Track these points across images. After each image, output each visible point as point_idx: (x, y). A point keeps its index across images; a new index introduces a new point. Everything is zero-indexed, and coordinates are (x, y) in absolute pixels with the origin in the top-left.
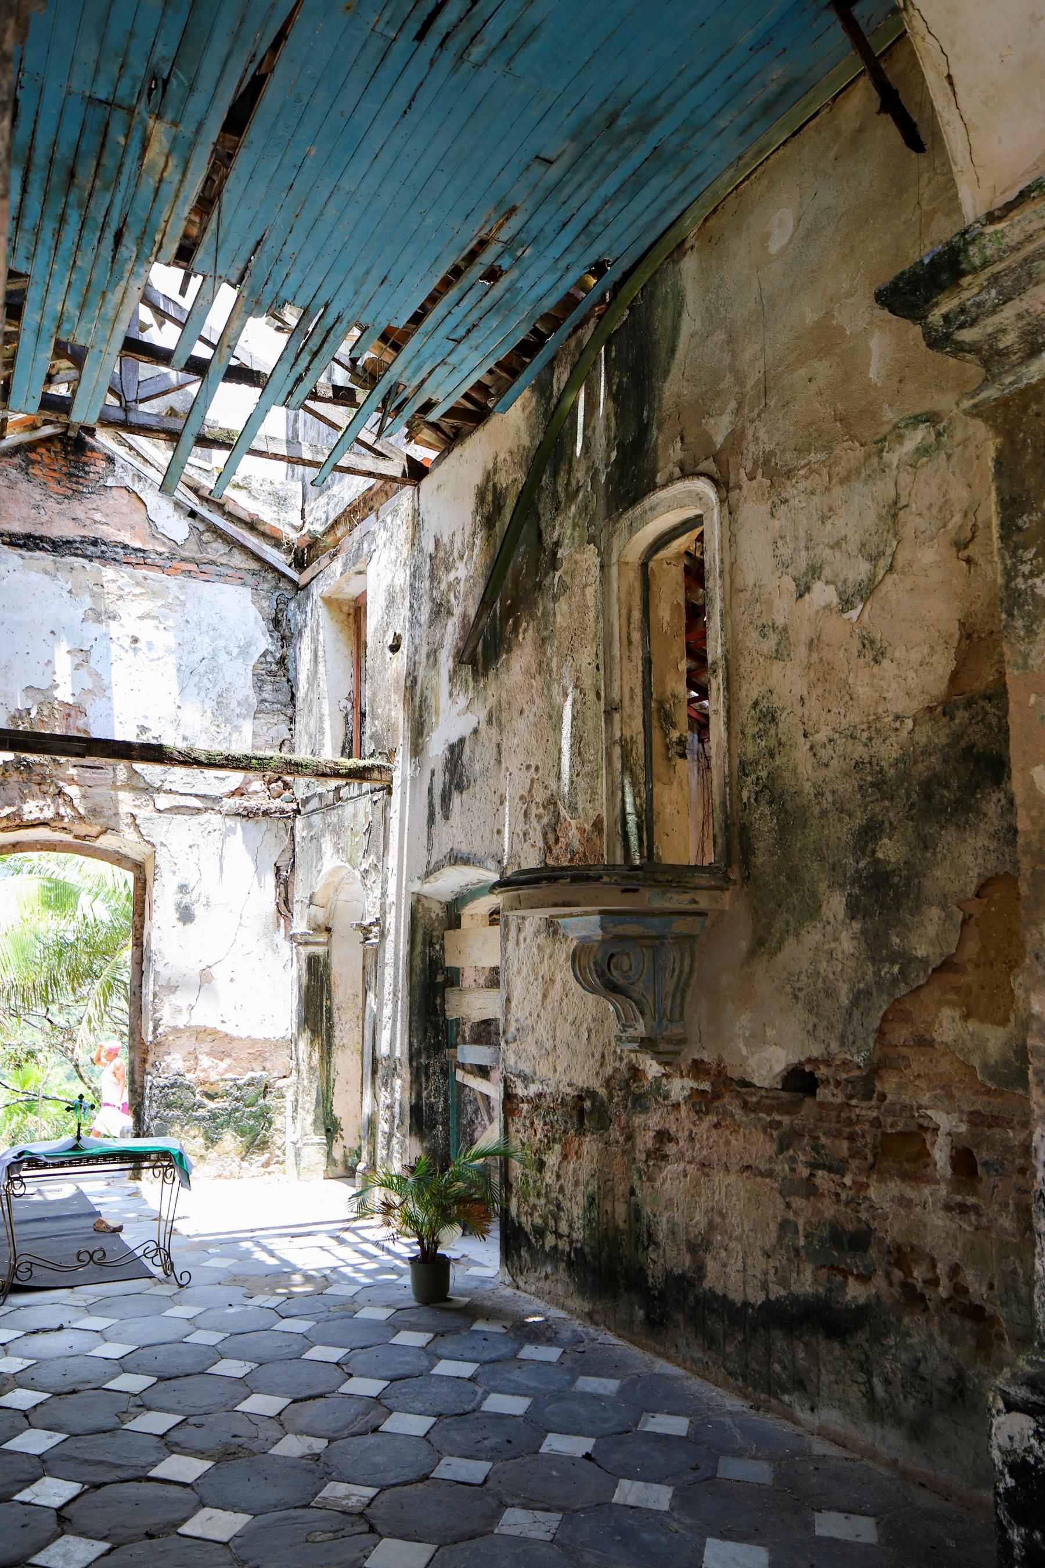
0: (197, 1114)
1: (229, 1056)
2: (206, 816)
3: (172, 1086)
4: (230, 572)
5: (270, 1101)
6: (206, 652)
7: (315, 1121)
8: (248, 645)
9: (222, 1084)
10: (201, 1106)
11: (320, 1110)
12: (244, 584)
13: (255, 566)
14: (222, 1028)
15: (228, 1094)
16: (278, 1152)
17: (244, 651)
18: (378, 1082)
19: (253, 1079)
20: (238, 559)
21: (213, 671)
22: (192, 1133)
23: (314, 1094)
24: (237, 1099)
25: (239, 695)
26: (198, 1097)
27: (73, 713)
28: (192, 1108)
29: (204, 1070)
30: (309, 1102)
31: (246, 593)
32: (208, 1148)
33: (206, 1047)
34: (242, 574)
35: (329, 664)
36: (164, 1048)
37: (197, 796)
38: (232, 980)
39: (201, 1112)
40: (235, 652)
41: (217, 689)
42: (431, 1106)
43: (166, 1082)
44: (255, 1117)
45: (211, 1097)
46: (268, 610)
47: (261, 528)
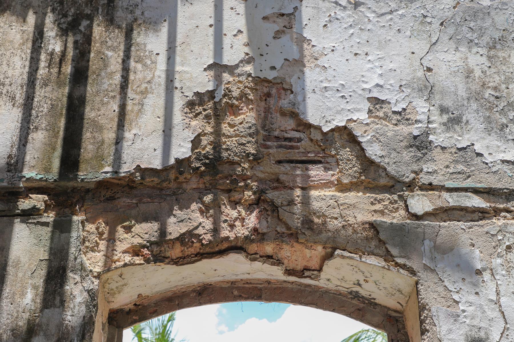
27: (274, 91)
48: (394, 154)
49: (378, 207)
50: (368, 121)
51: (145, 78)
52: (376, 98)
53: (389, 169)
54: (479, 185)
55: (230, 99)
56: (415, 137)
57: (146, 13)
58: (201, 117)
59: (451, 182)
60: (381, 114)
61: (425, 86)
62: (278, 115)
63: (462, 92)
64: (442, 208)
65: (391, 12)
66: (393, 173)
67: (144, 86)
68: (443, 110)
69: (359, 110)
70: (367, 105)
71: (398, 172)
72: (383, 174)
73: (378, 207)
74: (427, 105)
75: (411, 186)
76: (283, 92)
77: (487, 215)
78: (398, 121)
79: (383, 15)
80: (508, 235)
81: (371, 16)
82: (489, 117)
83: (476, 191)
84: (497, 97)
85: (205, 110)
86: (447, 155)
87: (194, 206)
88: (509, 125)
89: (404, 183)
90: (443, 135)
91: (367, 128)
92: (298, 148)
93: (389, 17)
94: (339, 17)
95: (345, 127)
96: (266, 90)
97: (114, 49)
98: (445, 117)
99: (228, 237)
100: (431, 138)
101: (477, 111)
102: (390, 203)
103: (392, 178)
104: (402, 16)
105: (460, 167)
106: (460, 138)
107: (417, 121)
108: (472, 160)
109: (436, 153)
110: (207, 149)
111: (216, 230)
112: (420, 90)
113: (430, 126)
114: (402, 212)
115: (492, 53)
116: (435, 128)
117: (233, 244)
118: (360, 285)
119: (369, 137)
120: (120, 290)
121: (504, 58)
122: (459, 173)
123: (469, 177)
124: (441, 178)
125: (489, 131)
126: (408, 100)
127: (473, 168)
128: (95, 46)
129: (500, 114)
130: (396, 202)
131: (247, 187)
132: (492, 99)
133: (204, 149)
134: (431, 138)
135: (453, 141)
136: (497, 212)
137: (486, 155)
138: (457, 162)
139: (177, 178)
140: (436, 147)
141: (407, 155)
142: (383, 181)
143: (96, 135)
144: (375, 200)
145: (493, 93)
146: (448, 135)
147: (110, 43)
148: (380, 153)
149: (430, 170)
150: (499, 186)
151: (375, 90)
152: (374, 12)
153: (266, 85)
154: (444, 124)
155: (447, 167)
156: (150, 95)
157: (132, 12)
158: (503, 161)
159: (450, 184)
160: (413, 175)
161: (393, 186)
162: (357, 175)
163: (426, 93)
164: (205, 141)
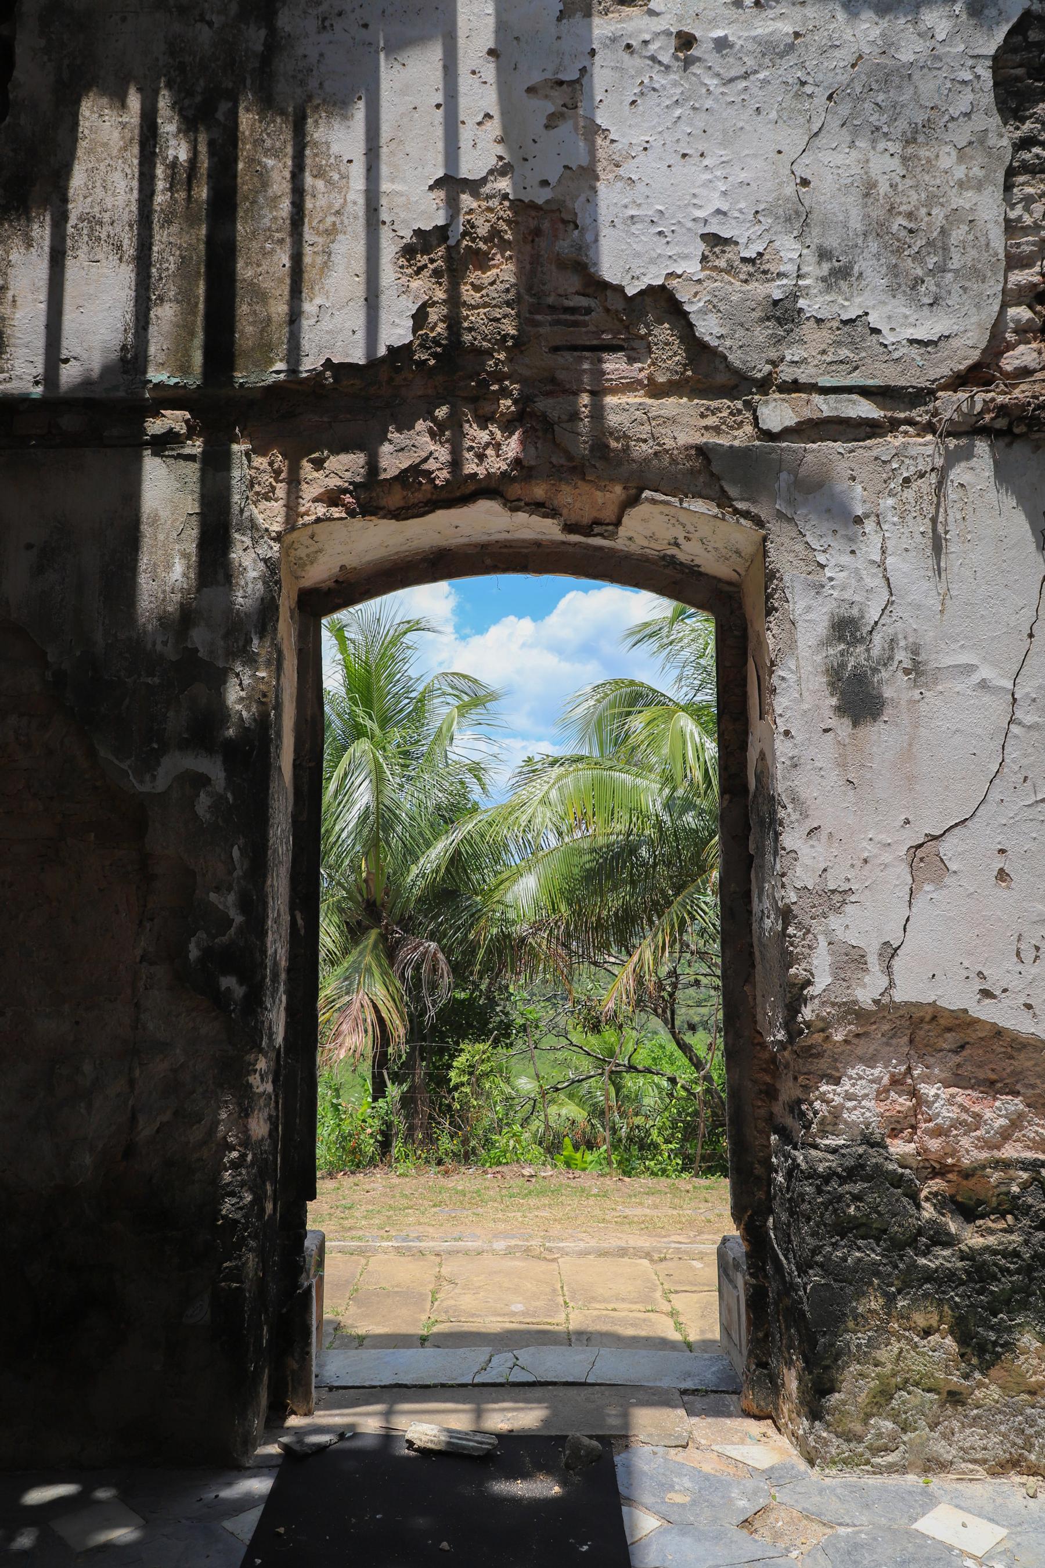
2: (895, 441)
3: (853, 1173)
9: (995, 1177)
14: (987, 1012)
22: (920, 1320)
26: (928, 1212)
27: (546, 225)
28: (912, 1242)
29: (938, 1132)
36: (823, 1064)
38: (1002, 875)
39: (941, 1258)
43: (831, 1162)
45: (969, 1212)
48: (740, 333)
49: (712, 421)
50: (701, 276)
51: (330, 206)
52: (715, 235)
53: (731, 357)
54: (870, 382)
55: (473, 240)
56: (776, 303)
57: (326, 84)
58: (426, 273)
59: (827, 377)
60: (722, 263)
61: (797, 212)
62: (553, 267)
63: (856, 224)
64: (810, 420)
65: (746, 76)
66: (737, 364)
67: (330, 219)
68: (824, 255)
69: (686, 257)
70: (701, 247)
71: (744, 363)
72: (722, 367)
73: (712, 421)
74: (798, 246)
75: (764, 385)
76: (561, 226)
77: (878, 430)
78: (750, 275)
79: (732, 80)
80: (907, 461)
81: (712, 82)
82: (896, 266)
83: (865, 392)
84: (911, 231)
85: (432, 261)
86: (825, 333)
87: (421, 425)
88: (926, 279)
89: (754, 380)
90: (820, 299)
91: (698, 287)
92: (585, 324)
93: (744, 84)
94: (657, 86)
95: (663, 287)
96: (532, 224)
97: (275, 153)
98: (826, 267)
99: (476, 474)
100: (802, 303)
101: (877, 256)
102: (731, 414)
103: (736, 372)
104: (765, 82)
105: (844, 353)
106: (846, 303)
107: (780, 275)
108: (863, 340)
109: (808, 329)
110: (438, 329)
111: (456, 463)
112: (788, 220)
113: (800, 283)
114: (749, 429)
115: (910, 150)
116: (807, 287)
117: (484, 484)
118: (677, 545)
119: (701, 304)
120: (312, 559)
121: (929, 161)
122: (841, 362)
123: (856, 368)
124: (812, 371)
125: (893, 290)
126: (767, 238)
127: (864, 354)
128: (246, 149)
129: (913, 261)
130: (739, 412)
131: (505, 393)
132: (903, 233)
133: (432, 329)
134: (802, 303)
135: (836, 309)
136: (894, 425)
137: (885, 331)
138: (838, 343)
139: (391, 379)
140: (808, 319)
141: (761, 334)
142: (721, 378)
143: (257, 308)
144: (707, 409)
145: (905, 223)
146: (828, 298)
147: (268, 143)
148: (717, 331)
149: (796, 359)
150: (902, 382)
151: (713, 220)
152: (718, 75)
153: (533, 213)
154: (824, 279)
155: (824, 352)
156: (340, 237)
157: (302, 83)
158: (912, 342)
159: (825, 381)
160: (769, 367)
161: (736, 386)
162: (679, 368)
163: (797, 225)
164: (434, 315)
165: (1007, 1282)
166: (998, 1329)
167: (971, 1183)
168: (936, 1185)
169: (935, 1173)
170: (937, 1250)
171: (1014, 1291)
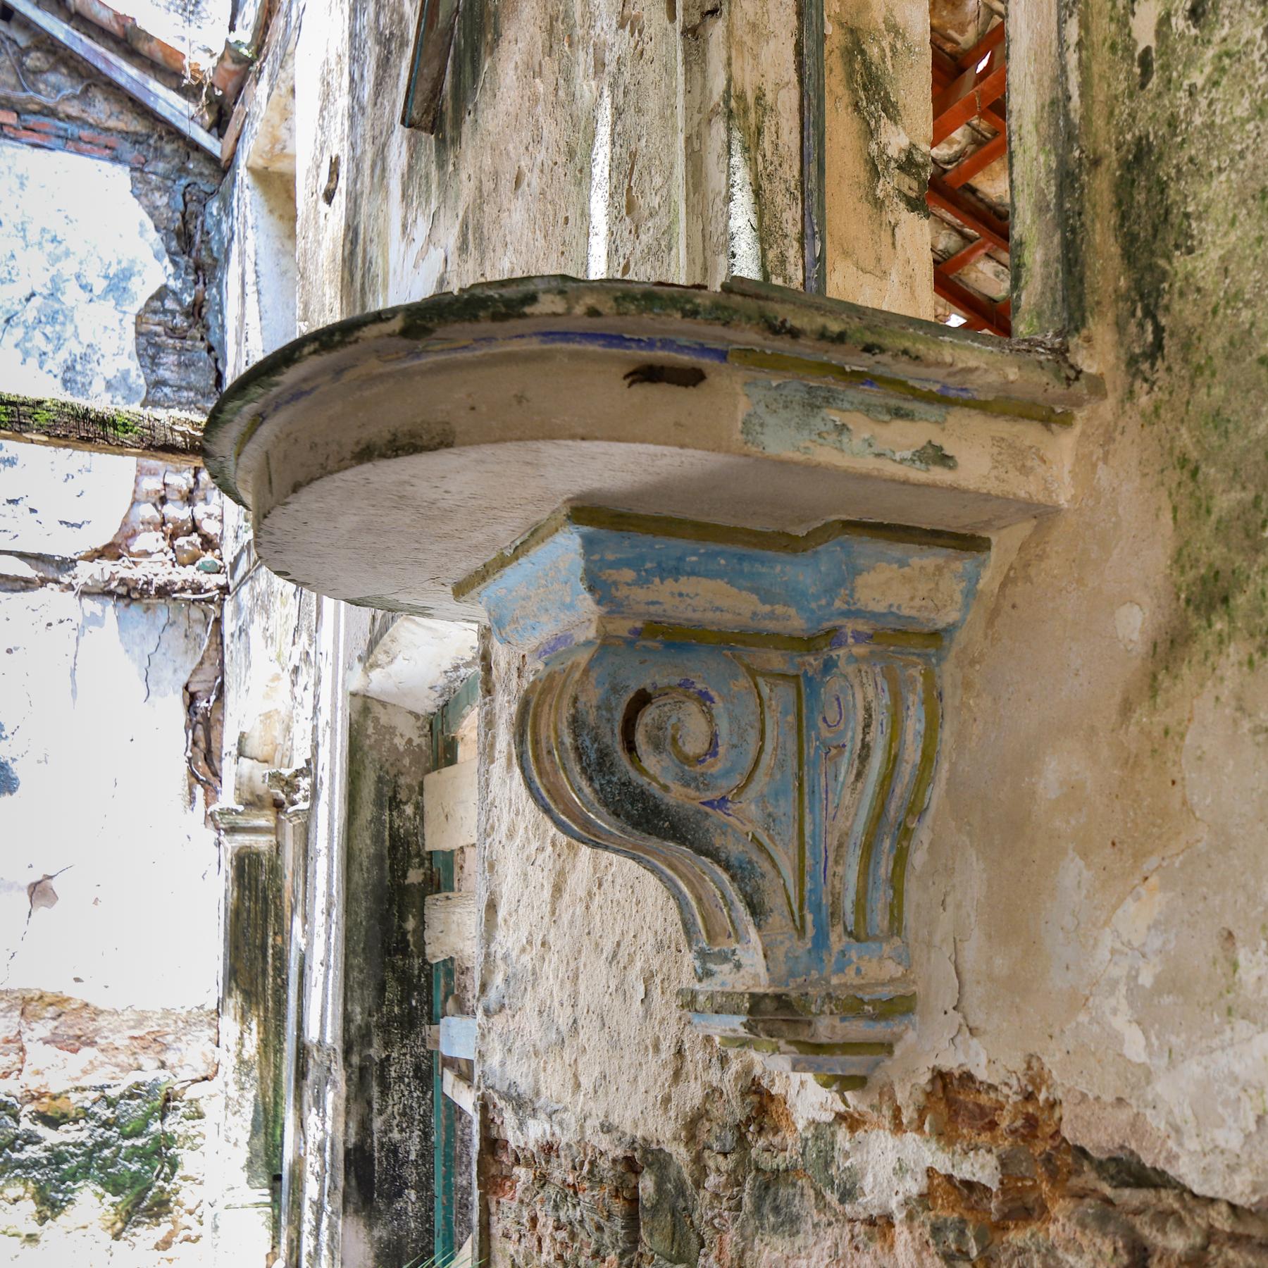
0: (22, 1156)
1: (92, 1043)
4: (86, 133)
5: (173, 1124)
6: (40, 282)
7: (250, 1164)
8: (126, 275)
9: (74, 1097)
10: (32, 1139)
11: (260, 1142)
12: (116, 159)
13: (136, 125)
15: (87, 1114)
16: (187, 1220)
17: (118, 285)
18: (308, 1096)
19: (138, 1085)
20: (101, 111)
21: (53, 319)
23: (248, 1112)
24: (106, 1124)
25: (109, 369)
26: (25, 1124)
30: (241, 1126)
31: (121, 176)
32: (43, 1219)
33: (43, 1029)
34: (113, 140)
35: (266, 300)
37: (22, 556)
39: (31, 1152)
40: (100, 286)
41: (63, 355)
42: (393, 1150)
44: (135, 1153)
45: (53, 1122)
46: (166, 213)
47: (144, 47)
115: (68, 375)
121: (83, 385)
136: (44, 582)
165: (74, 1163)
166: (65, 1192)
167: (58, 1102)
168: (29, 1108)
169: (33, 1098)
170: (28, 1147)
171: (79, 1167)
